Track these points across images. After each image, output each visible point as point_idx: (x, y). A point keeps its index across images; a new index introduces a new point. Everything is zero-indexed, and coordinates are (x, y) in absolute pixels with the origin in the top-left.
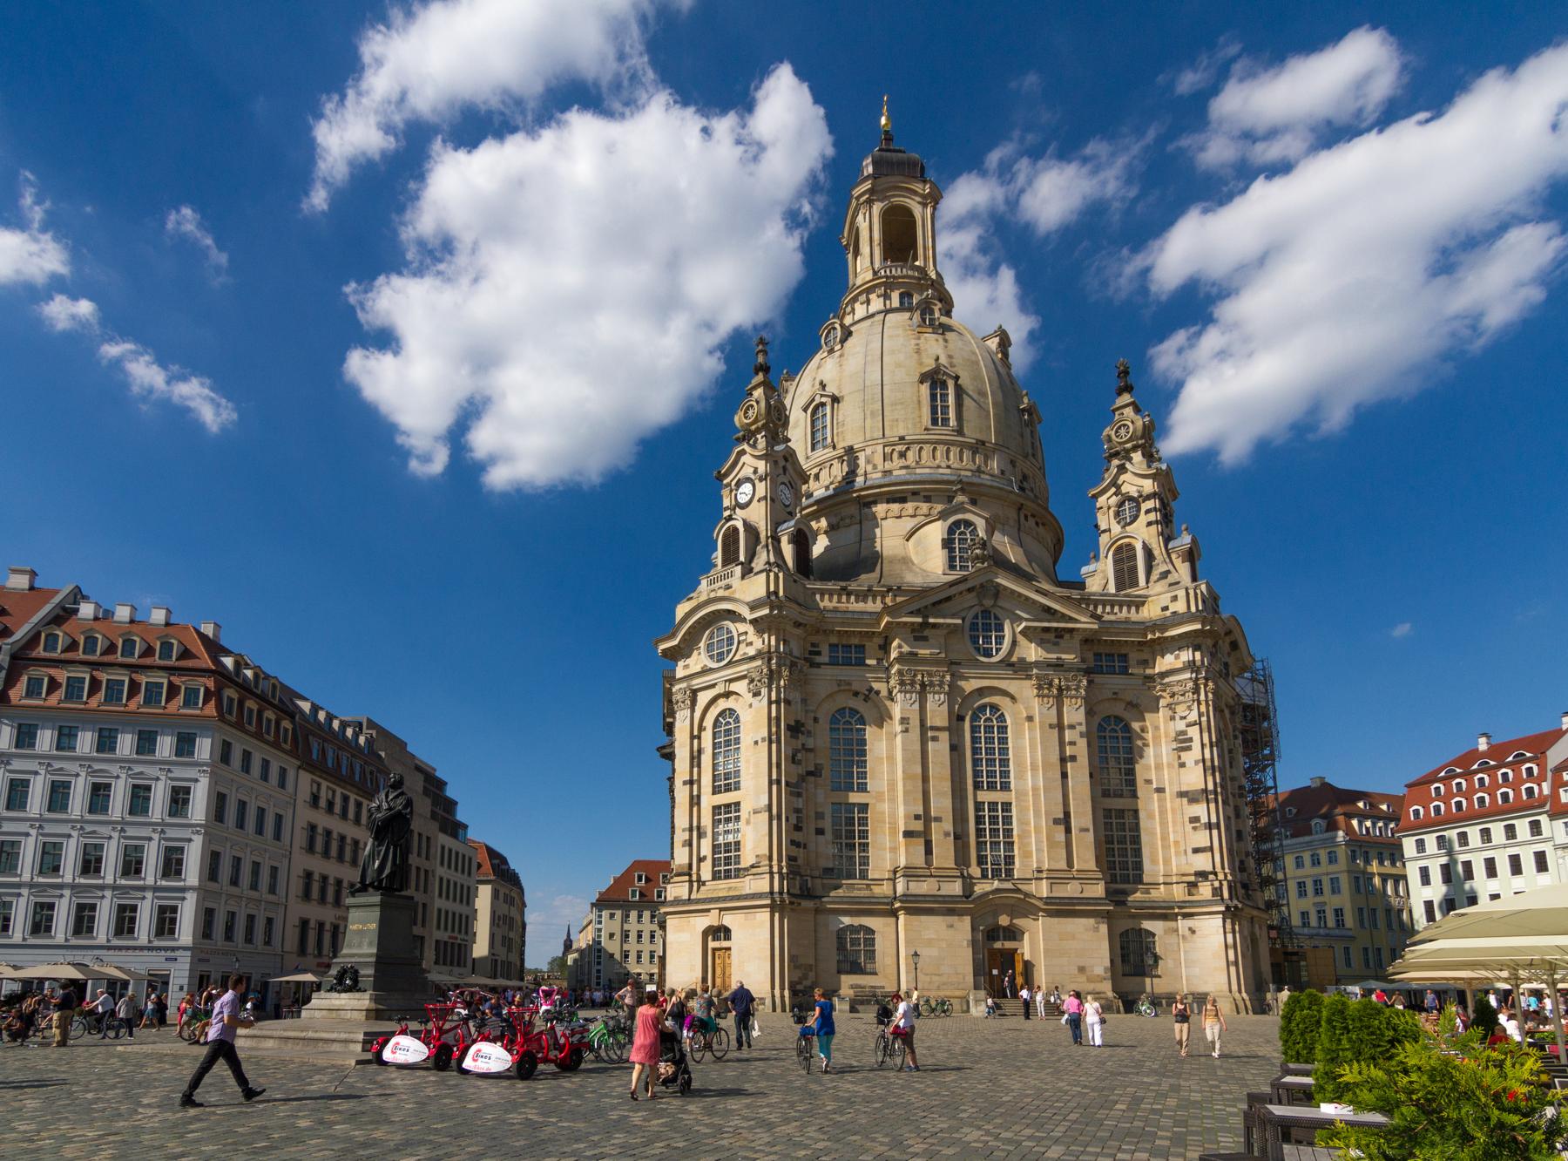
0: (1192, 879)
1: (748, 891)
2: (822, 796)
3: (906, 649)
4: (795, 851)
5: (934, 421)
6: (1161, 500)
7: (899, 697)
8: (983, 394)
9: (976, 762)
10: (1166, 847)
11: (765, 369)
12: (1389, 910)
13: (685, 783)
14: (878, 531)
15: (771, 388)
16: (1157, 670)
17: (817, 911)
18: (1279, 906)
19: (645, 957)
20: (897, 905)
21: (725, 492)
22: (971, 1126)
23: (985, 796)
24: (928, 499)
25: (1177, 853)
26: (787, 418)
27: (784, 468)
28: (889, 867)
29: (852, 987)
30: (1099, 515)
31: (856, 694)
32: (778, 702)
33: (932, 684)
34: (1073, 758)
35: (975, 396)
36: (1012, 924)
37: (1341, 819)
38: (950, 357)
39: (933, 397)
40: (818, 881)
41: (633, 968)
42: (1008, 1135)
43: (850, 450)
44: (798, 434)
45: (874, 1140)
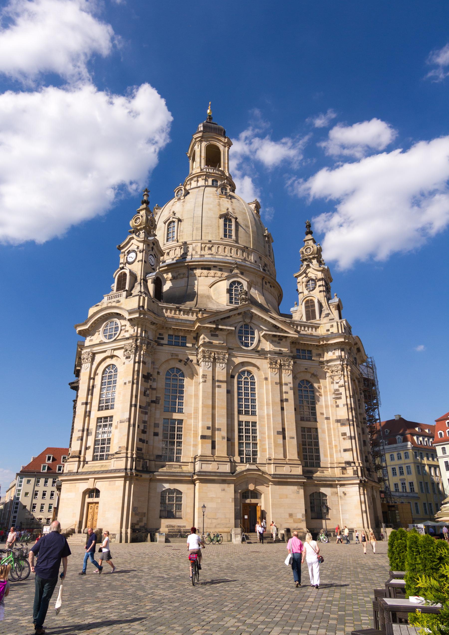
0: (344, 465)
1: (112, 468)
2: (159, 415)
3: (207, 340)
4: (141, 445)
5: (225, 236)
6: (325, 282)
7: (202, 364)
8: (248, 227)
9: (239, 400)
10: (331, 448)
11: (147, 202)
12: (433, 483)
13: (83, 404)
14: (196, 282)
15: (148, 211)
16: (325, 359)
17: (151, 480)
18: (384, 480)
19: (46, 508)
20: (195, 477)
21: (121, 256)
22: (230, 616)
23: (243, 418)
24: (221, 270)
25: (336, 451)
26: (156, 226)
27: (153, 248)
28: (192, 455)
29: (167, 526)
30: (298, 285)
31: (180, 361)
32: (139, 362)
33: (219, 359)
34: (287, 400)
35: (244, 227)
36: (255, 489)
37: (409, 436)
38: (233, 209)
39: (225, 225)
40: (153, 462)
41: (37, 514)
42: (249, 621)
43: (185, 244)
44: (160, 233)
45: (173, 629)
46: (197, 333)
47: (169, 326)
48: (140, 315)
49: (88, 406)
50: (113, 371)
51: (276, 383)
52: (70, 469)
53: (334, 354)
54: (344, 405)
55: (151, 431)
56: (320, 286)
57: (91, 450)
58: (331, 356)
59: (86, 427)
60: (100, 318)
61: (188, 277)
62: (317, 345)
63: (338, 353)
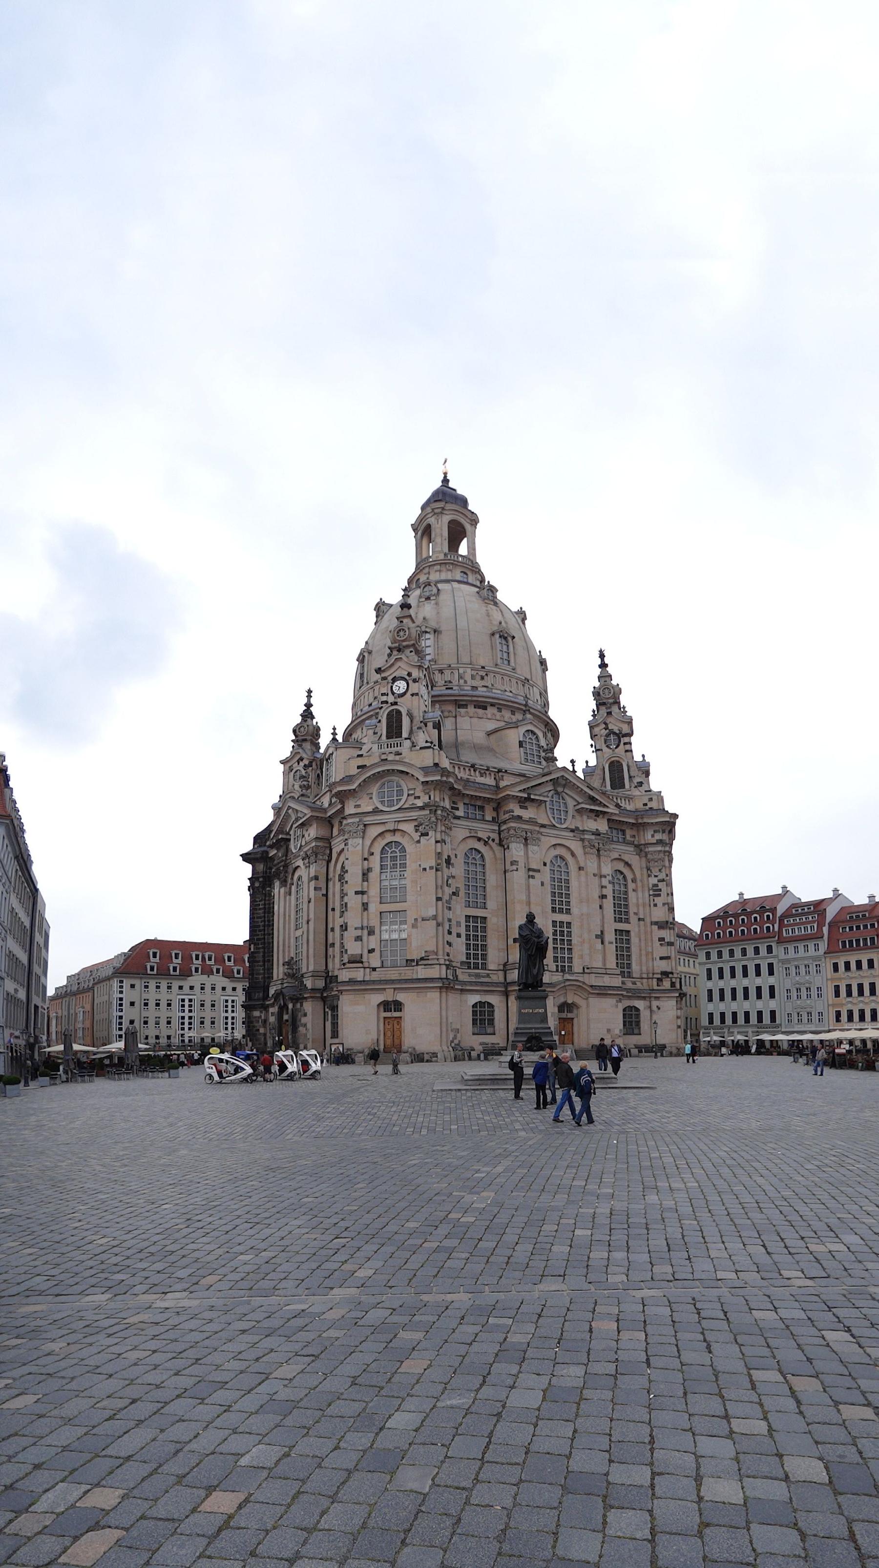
1: (420, 977)
13: (357, 893)
46: (499, 803)
47: (468, 792)
48: (442, 776)
49: (365, 896)
51: (595, 875)
57: (377, 953)
59: (365, 924)
60: (374, 775)
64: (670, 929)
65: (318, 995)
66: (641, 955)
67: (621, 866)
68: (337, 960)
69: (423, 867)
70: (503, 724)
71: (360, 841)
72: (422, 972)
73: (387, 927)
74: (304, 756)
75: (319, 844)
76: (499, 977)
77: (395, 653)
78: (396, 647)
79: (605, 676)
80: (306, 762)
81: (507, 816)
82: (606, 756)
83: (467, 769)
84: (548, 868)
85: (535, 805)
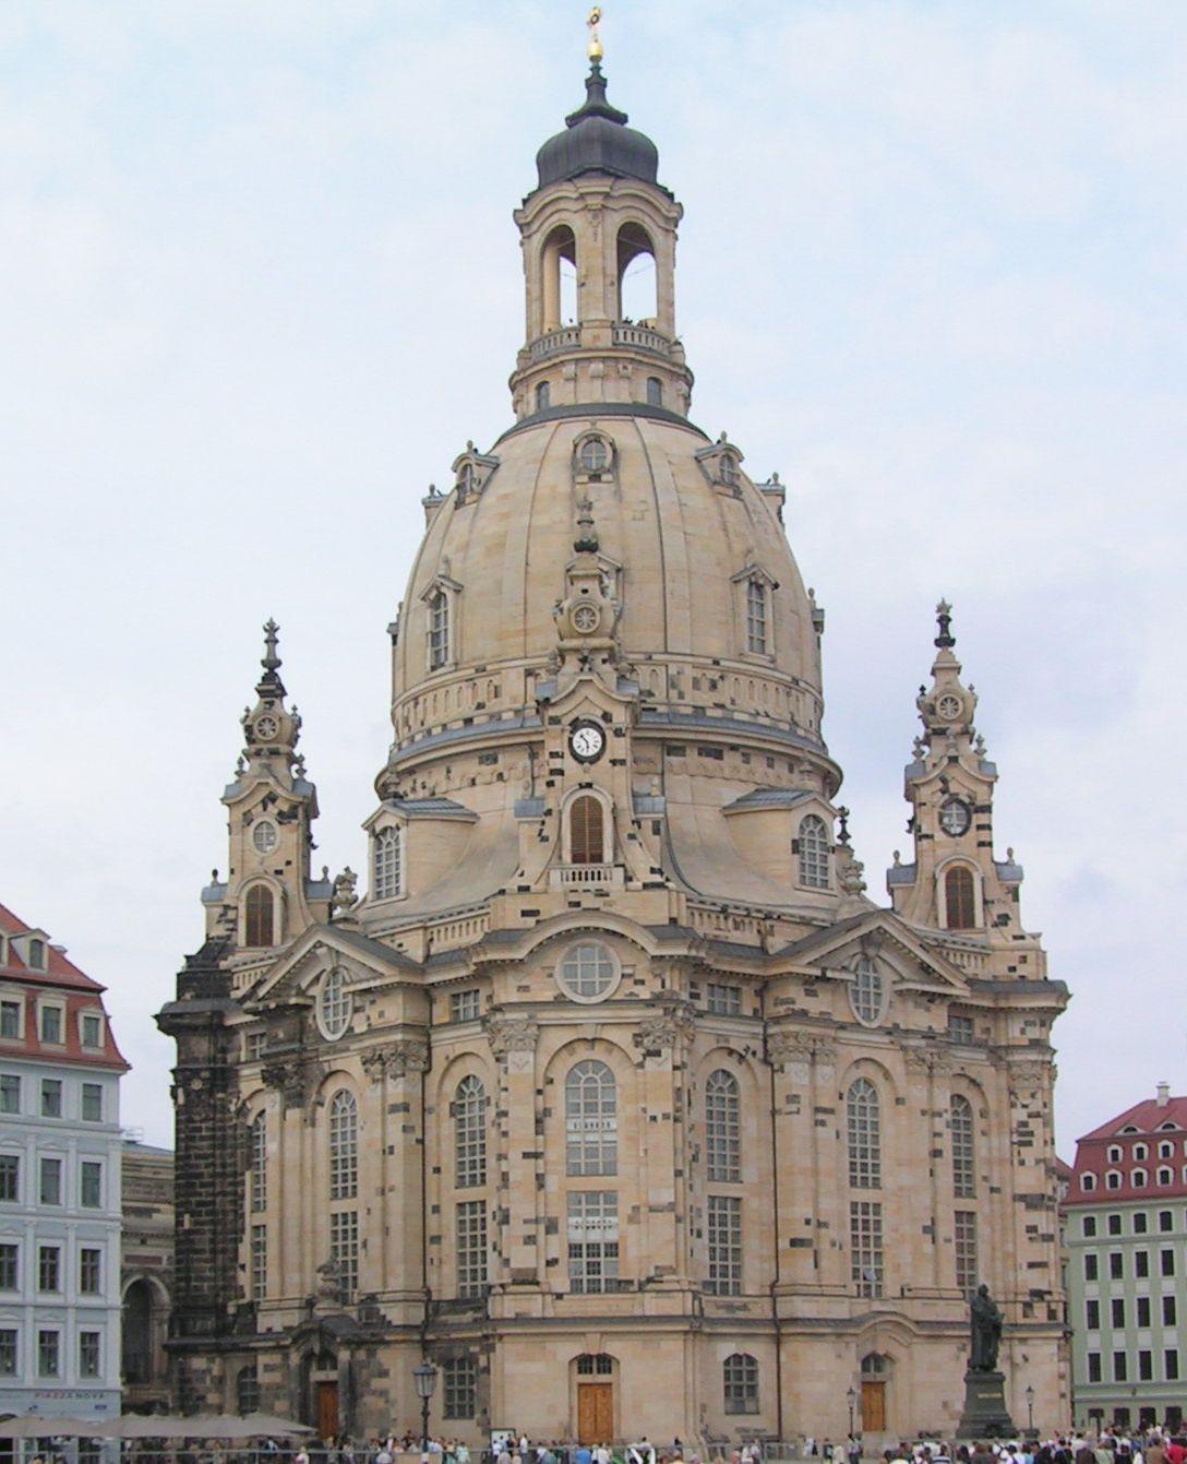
0: (1027, 1299)
1: (648, 1313)
13: (526, 1155)
48: (690, 948)
49: (540, 1162)
50: (597, 1077)
51: (923, 1113)
52: (518, 1310)
53: (1023, 1031)
54: (1038, 1162)
55: (695, 1227)
56: (979, 827)
58: (1014, 1038)
59: (542, 1215)
61: (663, 774)
62: (989, 1009)
63: (1034, 1033)
64: (1050, 1208)
65: (417, 1337)
66: (993, 1260)
67: (963, 1088)
68: (450, 1269)
69: (650, 1113)
70: (752, 788)
71: (531, 1057)
72: (651, 1305)
73: (580, 1220)
74: (280, 791)
75: (409, 1037)
76: (761, 1309)
77: (572, 664)
78: (576, 650)
79: (945, 669)
80: (285, 808)
81: (782, 1010)
82: (940, 852)
83: (713, 916)
84: (845, 1102)
85: (829, 986)
